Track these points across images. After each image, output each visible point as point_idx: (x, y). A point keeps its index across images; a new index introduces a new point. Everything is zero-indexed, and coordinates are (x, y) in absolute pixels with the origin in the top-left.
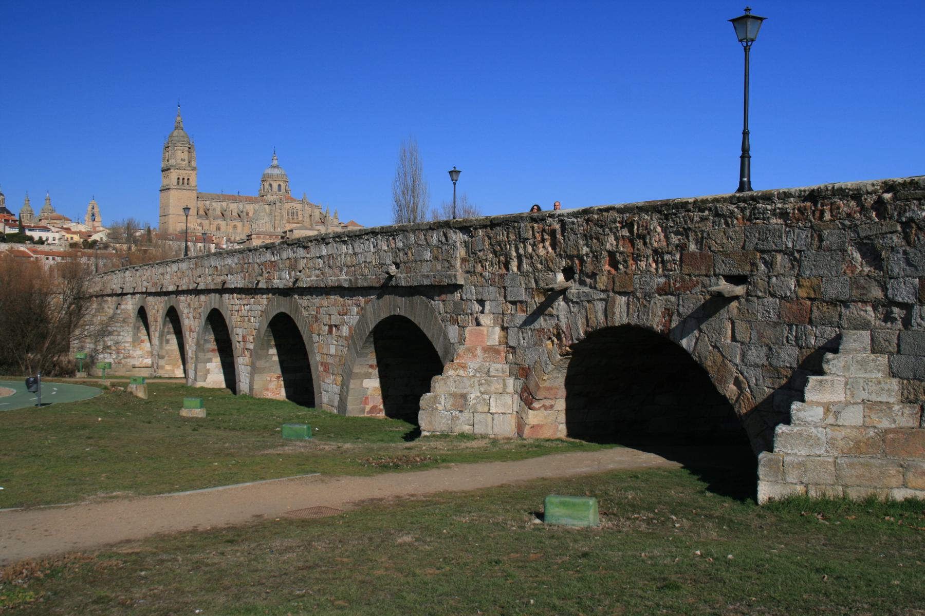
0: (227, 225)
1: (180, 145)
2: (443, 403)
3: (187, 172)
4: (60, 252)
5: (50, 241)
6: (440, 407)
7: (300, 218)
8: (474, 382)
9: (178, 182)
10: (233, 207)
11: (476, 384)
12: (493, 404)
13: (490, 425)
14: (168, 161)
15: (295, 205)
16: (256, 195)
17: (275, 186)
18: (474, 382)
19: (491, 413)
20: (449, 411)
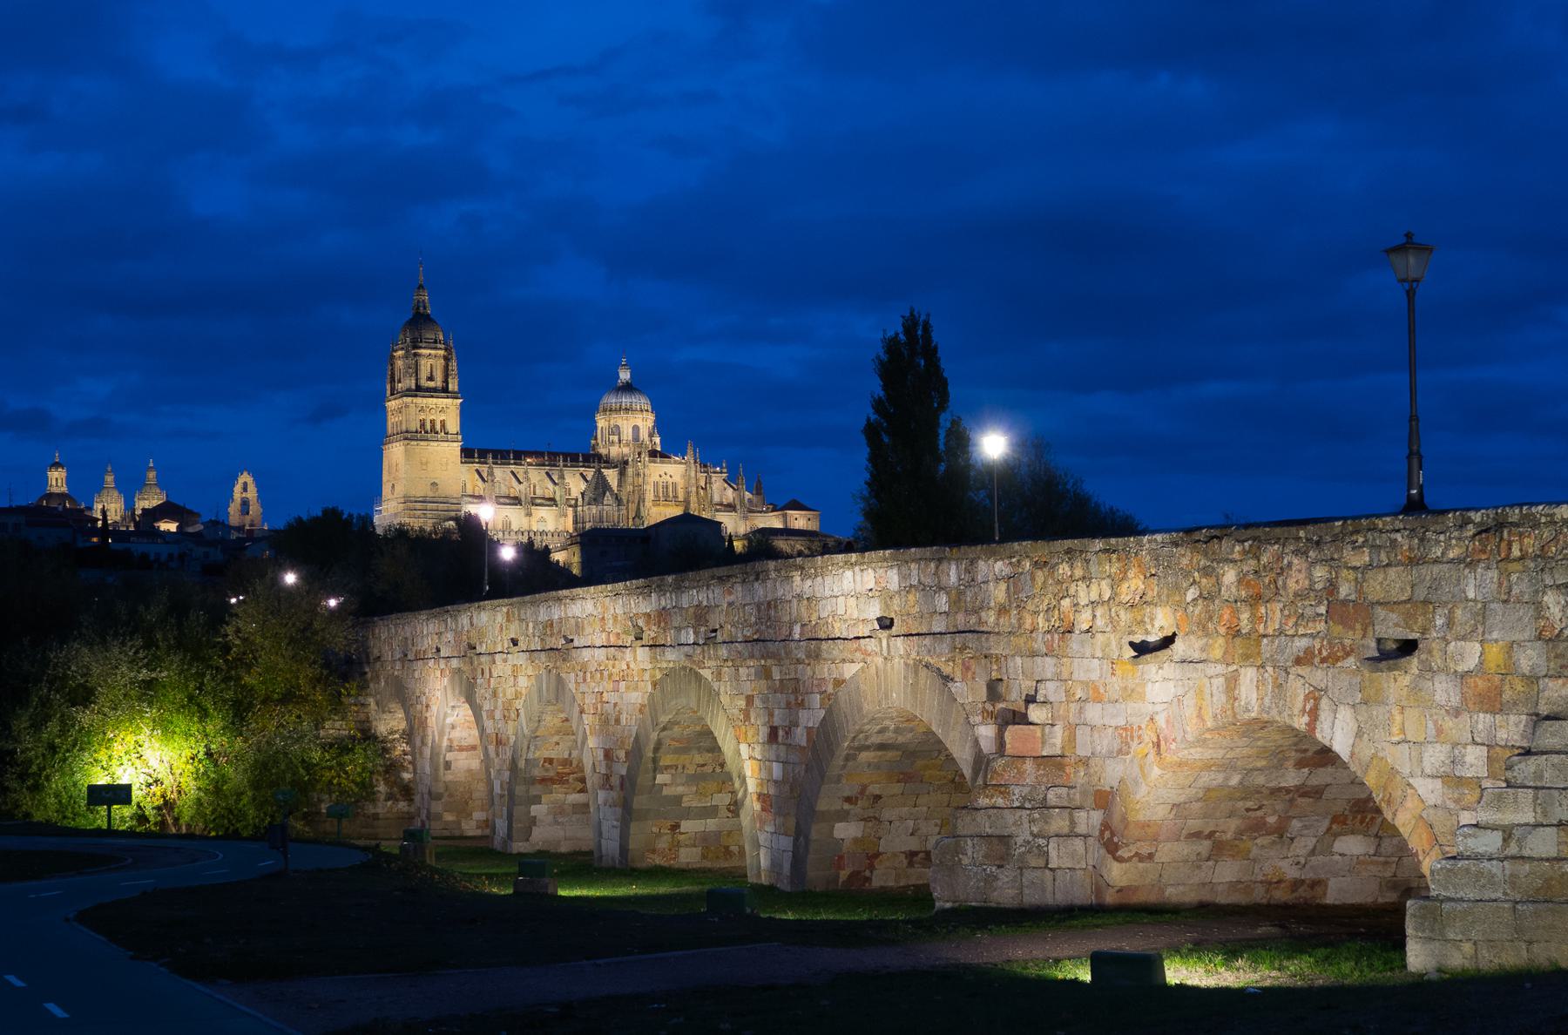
2: (970, 853)
6: (966, 861)
8: (1020, 817)
11: (1025, 820)
12: (1053, 854)
13: (1050, 888)
18: (1020, 817)
19: (1051, 869)
20: (981, 865)
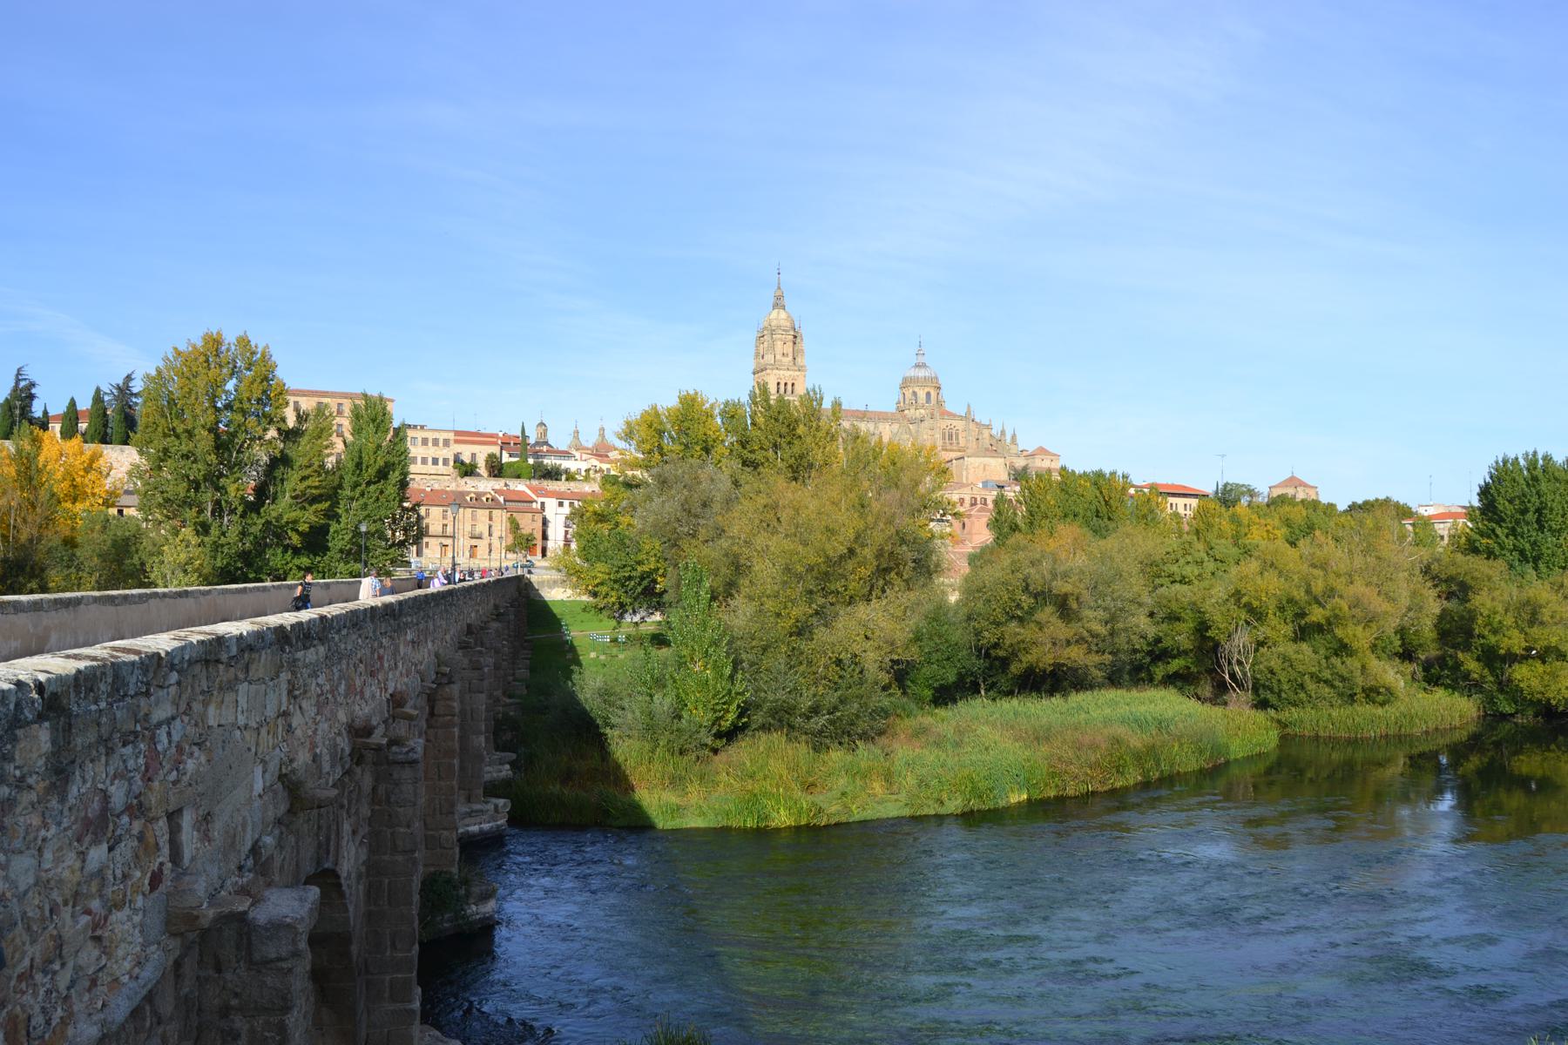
1: (780, 332)
3: (791, 373)
7: (962, 442)
9: (778, 389)
15: (954, 423)
16: (892, 408)
17: (922, 394)
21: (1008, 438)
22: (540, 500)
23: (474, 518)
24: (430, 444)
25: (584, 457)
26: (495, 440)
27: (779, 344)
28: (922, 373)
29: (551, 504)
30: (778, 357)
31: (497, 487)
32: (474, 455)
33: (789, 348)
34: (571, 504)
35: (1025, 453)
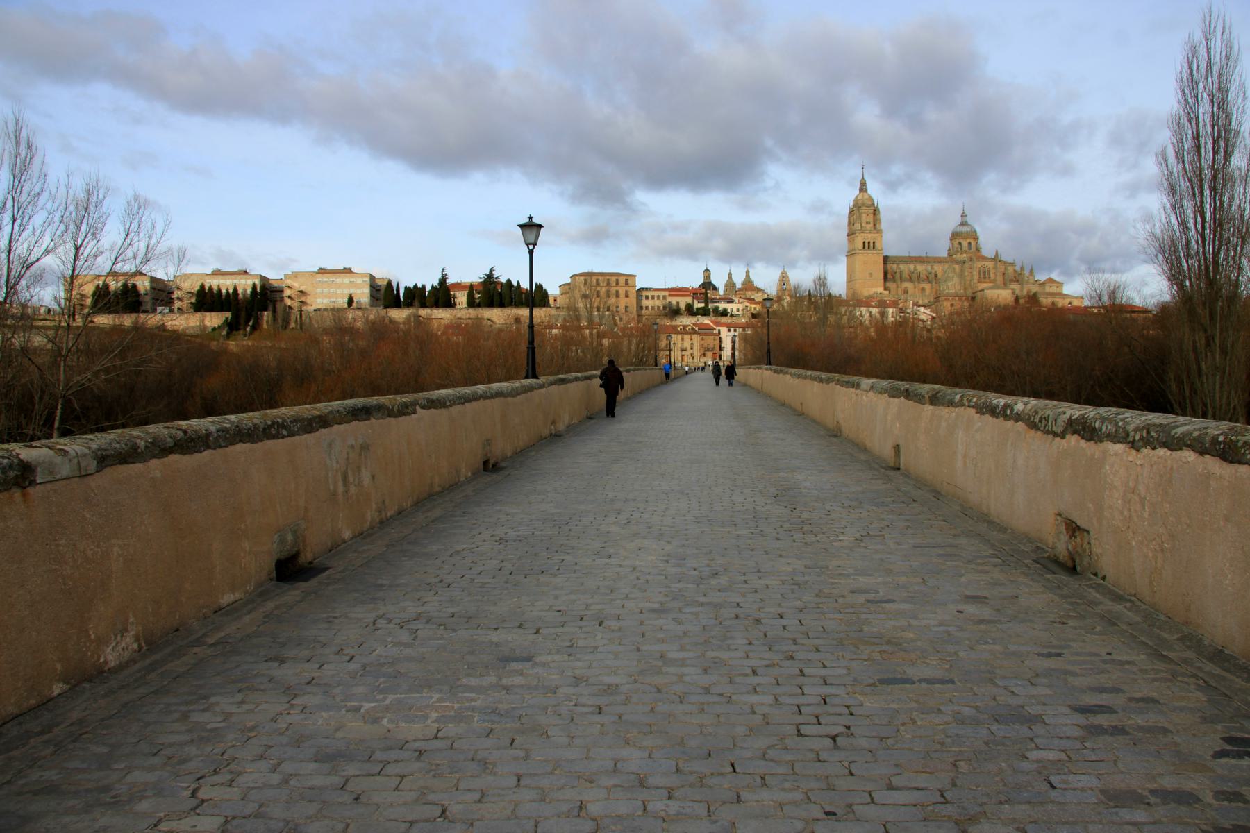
0: (915, 288)
3: (872, 235)
4: (743, 323)
5: (735, 312)
7: (992, 276)
10: (920, 268)
14: (853, 225)
15: (987, 263)
17: (965, 244)
21: (1027, 273)
22: (719, 328)
23: (683, 339)
24: (656, 299)
25: (741, 300)
26: (689, 293)
27: (864, 216)
28: (965, 229)
29: (724, 330)
30: (863, 225)
31: (693, 322)
32: (678, 303)
33: (871, 219)
34: (735, 331)
35: (1039, 283)
